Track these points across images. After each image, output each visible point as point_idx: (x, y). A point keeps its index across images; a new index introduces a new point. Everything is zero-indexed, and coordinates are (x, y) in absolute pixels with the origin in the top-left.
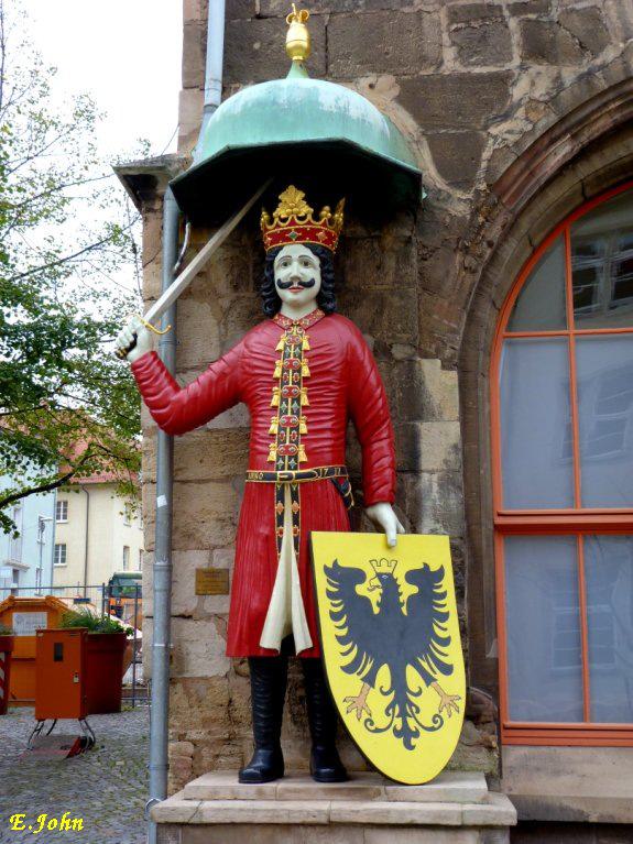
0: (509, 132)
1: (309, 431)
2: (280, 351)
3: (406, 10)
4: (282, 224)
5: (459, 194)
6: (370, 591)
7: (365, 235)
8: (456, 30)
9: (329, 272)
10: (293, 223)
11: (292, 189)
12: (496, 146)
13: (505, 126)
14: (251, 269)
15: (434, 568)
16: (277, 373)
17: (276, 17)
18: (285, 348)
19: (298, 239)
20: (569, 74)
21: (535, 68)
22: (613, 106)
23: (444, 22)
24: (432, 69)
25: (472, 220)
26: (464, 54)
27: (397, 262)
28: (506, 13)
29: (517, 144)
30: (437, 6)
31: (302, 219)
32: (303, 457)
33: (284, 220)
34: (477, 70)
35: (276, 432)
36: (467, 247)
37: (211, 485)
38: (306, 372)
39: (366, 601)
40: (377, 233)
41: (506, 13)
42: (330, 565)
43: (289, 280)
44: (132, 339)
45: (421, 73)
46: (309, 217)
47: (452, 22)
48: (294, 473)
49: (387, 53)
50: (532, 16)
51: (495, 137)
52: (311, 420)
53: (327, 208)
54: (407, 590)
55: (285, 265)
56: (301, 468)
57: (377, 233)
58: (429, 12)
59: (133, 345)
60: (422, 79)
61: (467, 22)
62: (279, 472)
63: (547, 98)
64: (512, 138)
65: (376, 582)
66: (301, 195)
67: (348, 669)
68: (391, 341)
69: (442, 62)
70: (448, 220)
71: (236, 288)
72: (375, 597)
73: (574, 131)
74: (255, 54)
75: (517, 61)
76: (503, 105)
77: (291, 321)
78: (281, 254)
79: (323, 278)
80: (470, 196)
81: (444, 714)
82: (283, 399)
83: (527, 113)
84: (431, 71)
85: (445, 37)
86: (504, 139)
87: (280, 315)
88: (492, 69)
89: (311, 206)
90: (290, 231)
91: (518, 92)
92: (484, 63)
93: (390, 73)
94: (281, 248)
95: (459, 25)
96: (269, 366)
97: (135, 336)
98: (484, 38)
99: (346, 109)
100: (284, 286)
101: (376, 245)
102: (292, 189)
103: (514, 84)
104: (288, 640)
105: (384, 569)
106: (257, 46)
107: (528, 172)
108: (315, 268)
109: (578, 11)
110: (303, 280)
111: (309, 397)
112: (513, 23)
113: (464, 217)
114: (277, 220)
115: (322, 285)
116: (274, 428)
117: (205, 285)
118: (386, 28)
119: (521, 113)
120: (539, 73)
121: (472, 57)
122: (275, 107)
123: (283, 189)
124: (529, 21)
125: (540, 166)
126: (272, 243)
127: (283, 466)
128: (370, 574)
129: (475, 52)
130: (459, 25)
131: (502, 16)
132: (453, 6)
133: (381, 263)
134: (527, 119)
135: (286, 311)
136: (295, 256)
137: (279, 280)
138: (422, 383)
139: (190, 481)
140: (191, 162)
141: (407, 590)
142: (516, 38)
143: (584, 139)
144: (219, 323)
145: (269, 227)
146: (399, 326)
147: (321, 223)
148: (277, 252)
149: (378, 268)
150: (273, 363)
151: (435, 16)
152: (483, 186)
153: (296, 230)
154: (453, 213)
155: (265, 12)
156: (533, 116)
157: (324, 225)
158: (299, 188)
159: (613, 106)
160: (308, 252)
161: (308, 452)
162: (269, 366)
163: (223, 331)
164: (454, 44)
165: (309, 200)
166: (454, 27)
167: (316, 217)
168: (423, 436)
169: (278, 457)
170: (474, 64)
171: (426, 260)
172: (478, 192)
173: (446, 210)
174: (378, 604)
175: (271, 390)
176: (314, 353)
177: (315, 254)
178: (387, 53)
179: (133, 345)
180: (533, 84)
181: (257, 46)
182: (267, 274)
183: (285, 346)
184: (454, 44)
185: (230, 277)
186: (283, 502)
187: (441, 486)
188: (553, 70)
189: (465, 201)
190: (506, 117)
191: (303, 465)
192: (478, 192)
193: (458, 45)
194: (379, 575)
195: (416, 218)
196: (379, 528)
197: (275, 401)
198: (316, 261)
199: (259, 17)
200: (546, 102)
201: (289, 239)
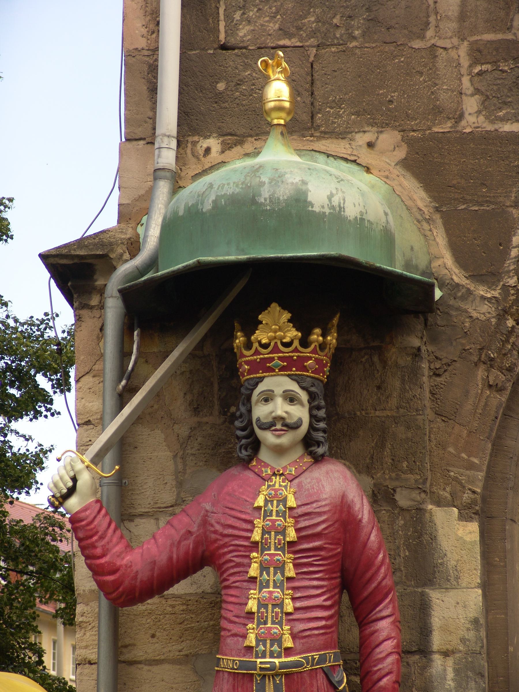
1: (296, 609)
2: (259, 508)
3: (417, 44)
5: (482, 291)
7: (362, 345)
9: (319, 408)
10: (276, 350)
11: (275, 307)
14: (216, 387)
16: (256, 536)
17: (245, 48)
18: (266, 505)
19: (282, 369)
23: (465, 62)
24: (449, 124)
25: (498, 324)
27: (403, 381)
30: (455, 41)
32: (289, 643)
33: (265, 346)
35: (255, 609)
36: (492, 360)
37: (167, 667)
38: (292, 535)
40: (376, 344)
43: (270, 420)
44: (70, 484)
45: (436, 129)
46: (296, 343)
47: (475, 62)
48: (277, 661)
49: (391, 102)
52: (298, 595)
53: (318, 331)
55: (266, 400)
56: (286, 656)
57: (376, 344)
58: (445, 49)
59: (72, 491)
60: (434, 137)
62: (259, 660)
66: (286, 316)
68: (397, 483)
69: (461, 116)
71: (196, 410)
74: (219, 97)
77: (272, 468)
78: (261, 387)
79: (311, 416)
80: (496, 293)
82: (264, 568)
84: (446, 127)
85: (466, 81)
87: (259, 461)
89: (297, 330)
90: (273, 359)
93: (395, 128)
94: (261, 379)
95: (484, 67)
96: (249, 527)
97: (74, 479)
99: (341, 208)
101: (376, 359)
102: (275, 307)
106: (221, 86)
108: (302, 404)
110: (288, 421)
111: (296, 566)
113: (488, 320)
114: (256, 345)
115: (311, 425)
116: (252, 605)
117: (156, 407)
118: (389, 68)
121: (500, 109)
122: (253, 208)
123: (264, 307)
126: (250, 372)
127: (264, 652)
129: (505, 103)
130: (484, 67)
133: (383, 382)
135: (264, 455)
136: (279, 391)
137: (258, 420)
138: (434, 538)
139: (140, 662)
144: (175, 456)
145: (245, 353)
146: (405, 464)
148: (257, 384)
149: (379, 388)
150: (251, 522)
151: (453, 54)
153: (280, 358)
154: (475, 315)
155: (232, 41)
157: (314, 351)
158: (284, 307)
160: (294, 387)
161: (294, 636)
162: (245, 526)
163: (180, 467)
164: (477, 91)
166: (477, 69)
167: (305, 343)
168: (435, 607)
169: (257, 641)
170: (504, 120)
171: (439, 375)
172: (505, 288)
175: (248, 557)
176: (300, 511)
177: (303, 388)
178: (391, 102)
179: (72, 491)
181: (221, 86)
182: (243, 409)
183: (266, 501)
184: (477, 91)
185: (189, 397)
187: (457, 671)
189: (489, 300)
191: (288, 651)
192: (505, 288)
193: (482, 94)
195: (426, 320)
197: (254, 571)
198: (304, 396)
199: (224, 47)
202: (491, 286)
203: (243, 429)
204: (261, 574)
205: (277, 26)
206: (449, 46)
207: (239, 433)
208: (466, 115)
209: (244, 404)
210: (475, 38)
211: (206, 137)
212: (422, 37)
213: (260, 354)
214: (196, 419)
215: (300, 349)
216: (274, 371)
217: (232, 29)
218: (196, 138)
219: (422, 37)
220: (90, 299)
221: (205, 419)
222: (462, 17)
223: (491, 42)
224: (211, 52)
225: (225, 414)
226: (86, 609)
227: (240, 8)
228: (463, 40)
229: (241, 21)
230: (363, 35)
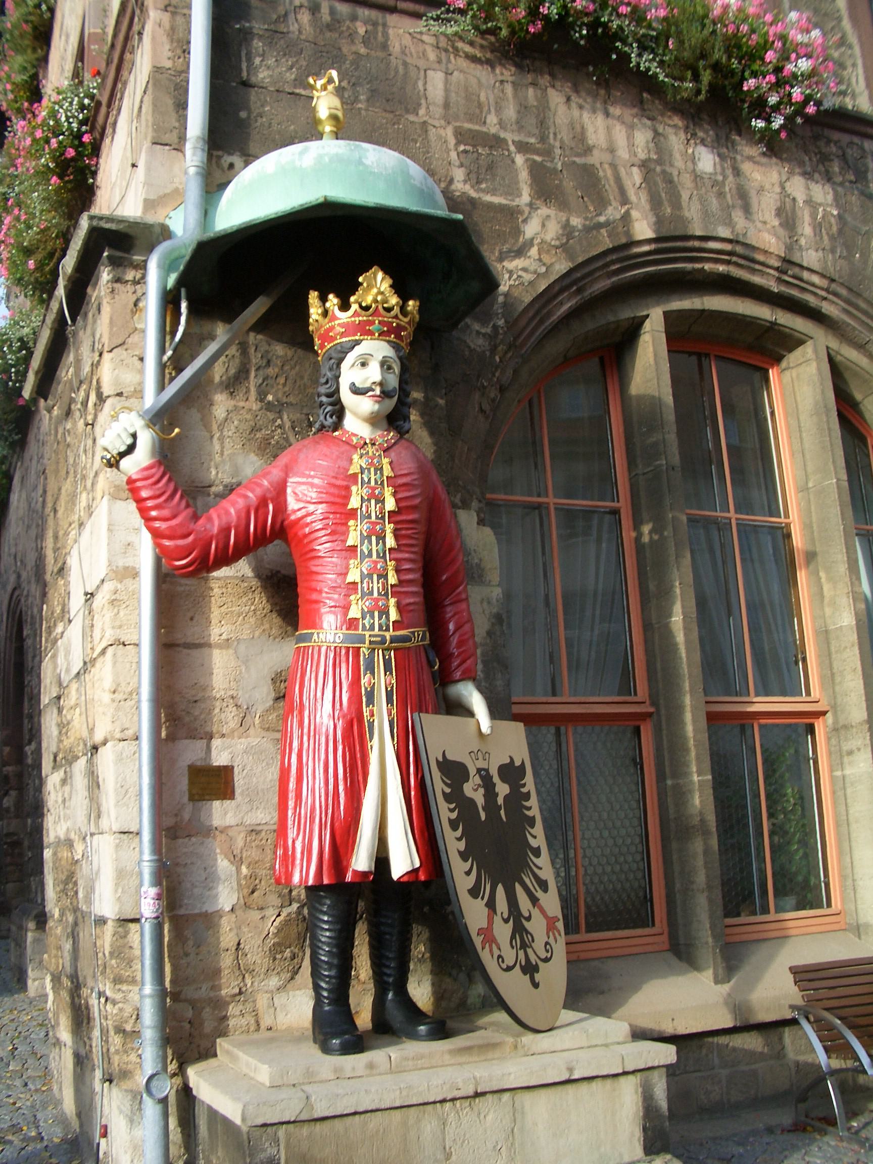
0: (525, 270)
2: (355, 476)
3: (412, 118)
6: (473, 790)
8: (465, 152)
10: (376, 313)
12: (512, 282)
13: (518, 263)
15: (518, 763)
17: (265, 88)
20: (576, 222)
21: (544, 211)
22: (614, 267)
23: (452, 141)
26: (475, 176)
28: (512, 148)
29: (531, 283)
30: (443, 122)
31: (385, 309)
34: (488, 198)
35: (358, 580)
39: (472, 802)
41: (512, 148)
42: (441, 759)
44: (129, 441)
46: (396, 310)
47: (458, 143)
50: (538, 159)
51: (511, 272)
54: (503, 789)
55: (363, 364)
58: (434, 127)
59: (131, 449)
61: (474, 146)
62: (367, 634)
63: (557, 243)
64: (527, 277)
65: (477, 778)
67: (474, 892)
70: (467, 353)
72: (479, 798)
73: (580, 284)
75: (525, 198)
76: (517, 240)
78: (358, 350)
80: (488, 330)
81: (552, 941)
83: (539, 254)
85: (453, 155)
86: (519, 277)
88: (503, 201)
90: (373, 323)
91: (531, 229)
92: (493, 192)
94: (358, 343)
95: (468, 148)
97: (134, 436)
98: (491, 167)
103: (525, 221)
104: (382, 861)
105: (481, 764)
107: (538, 318)
109: (578, 165)
112: (519, 160)
113: (484, 352)
114: (355, 307)
119: (534, 251)
120: (548, 216)
124: (535, 161)
125: (549, 314)
128: (472, 771)
131: (508, 150)
132: (460, 127)
134: (540, 260)
139: (178, 645)
140: (423, 190)
141: (503, 789)
142: (524, 175)
143: (587, 293)
152: (501, 322)
154: (472, 346)
156: (546, 259)
158: (386, 272)
159: (614, 267)
164: (462, 165)
165: (397, 288)
166: (462, 148)
170: (483, 191)
172: (495, 327)
173: (465, 342)
174: (484, 809)
179: (131, 449)
180: (543, 225)
186: (373, 673)
188: (563, 216)
189: (484, 335)
190: (520, 252)
194: (479, 771)
196: (462, 710)
200: (557, 247)
201: (370, 333)
203: (329, 395)
204: (362, 544)
205: (293, 76)
206: (437, 125)
207: (324, 399)
208: (455, 181)
209: (331, 369)
210: (458, 124)
211: (230, 154)
213: (359, 315)
214: (233, 403)
215: (400, 316)
216: (373, 334)
218: (220, 153)
220: (124, 273)
221: (242, 404)
222: (446, 105)
223: (470, 130)
224: (234, 84)
225: (261, 400)
226: (119, 586)
227: (259, 56)
228: (449, 123)
229: (261, 66)
230: (368, 100)
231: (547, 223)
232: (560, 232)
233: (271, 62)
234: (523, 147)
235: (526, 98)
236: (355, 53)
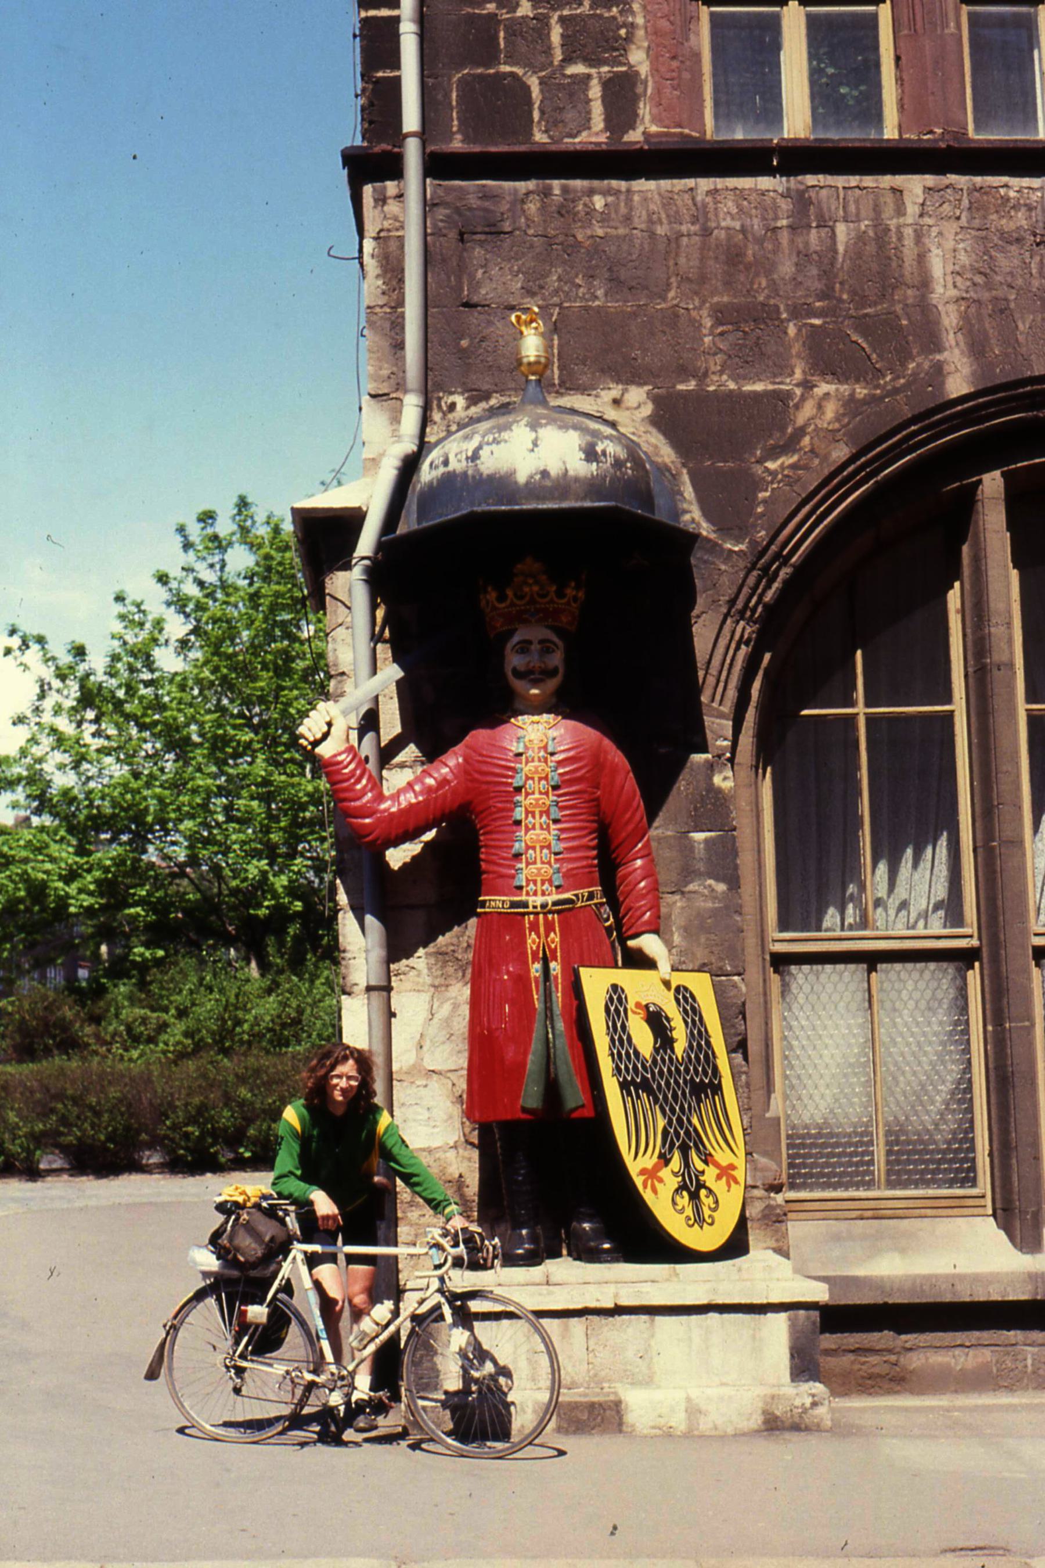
4: (518, 602)
8: (722, 334)
21: (823, 388)
47: (719, 322)
50: (817, 322)
63: (837, 426)
75: (798, 375)
84: (692, 385)
100: (518, 674)
120: (827, 394)
132: (718, 303)
147: (564, 601)
155: (475, 299)
157: (568, 603)
166: (720, 329)
167: (560, 594)
199: (466, 305)
202: (738, 540)
205: (519, 285)
210: (716, 299)
211: (452, 393)
212: (664, 299)
217: (475, 286)
219: (664, 299)
227: (482, 267)
230: (606, 295)
231: (824, 403)
232: (841, 411)
233: (495, 271)
234: (798, 312)
235: (807, 244)
236: (592, 237)
